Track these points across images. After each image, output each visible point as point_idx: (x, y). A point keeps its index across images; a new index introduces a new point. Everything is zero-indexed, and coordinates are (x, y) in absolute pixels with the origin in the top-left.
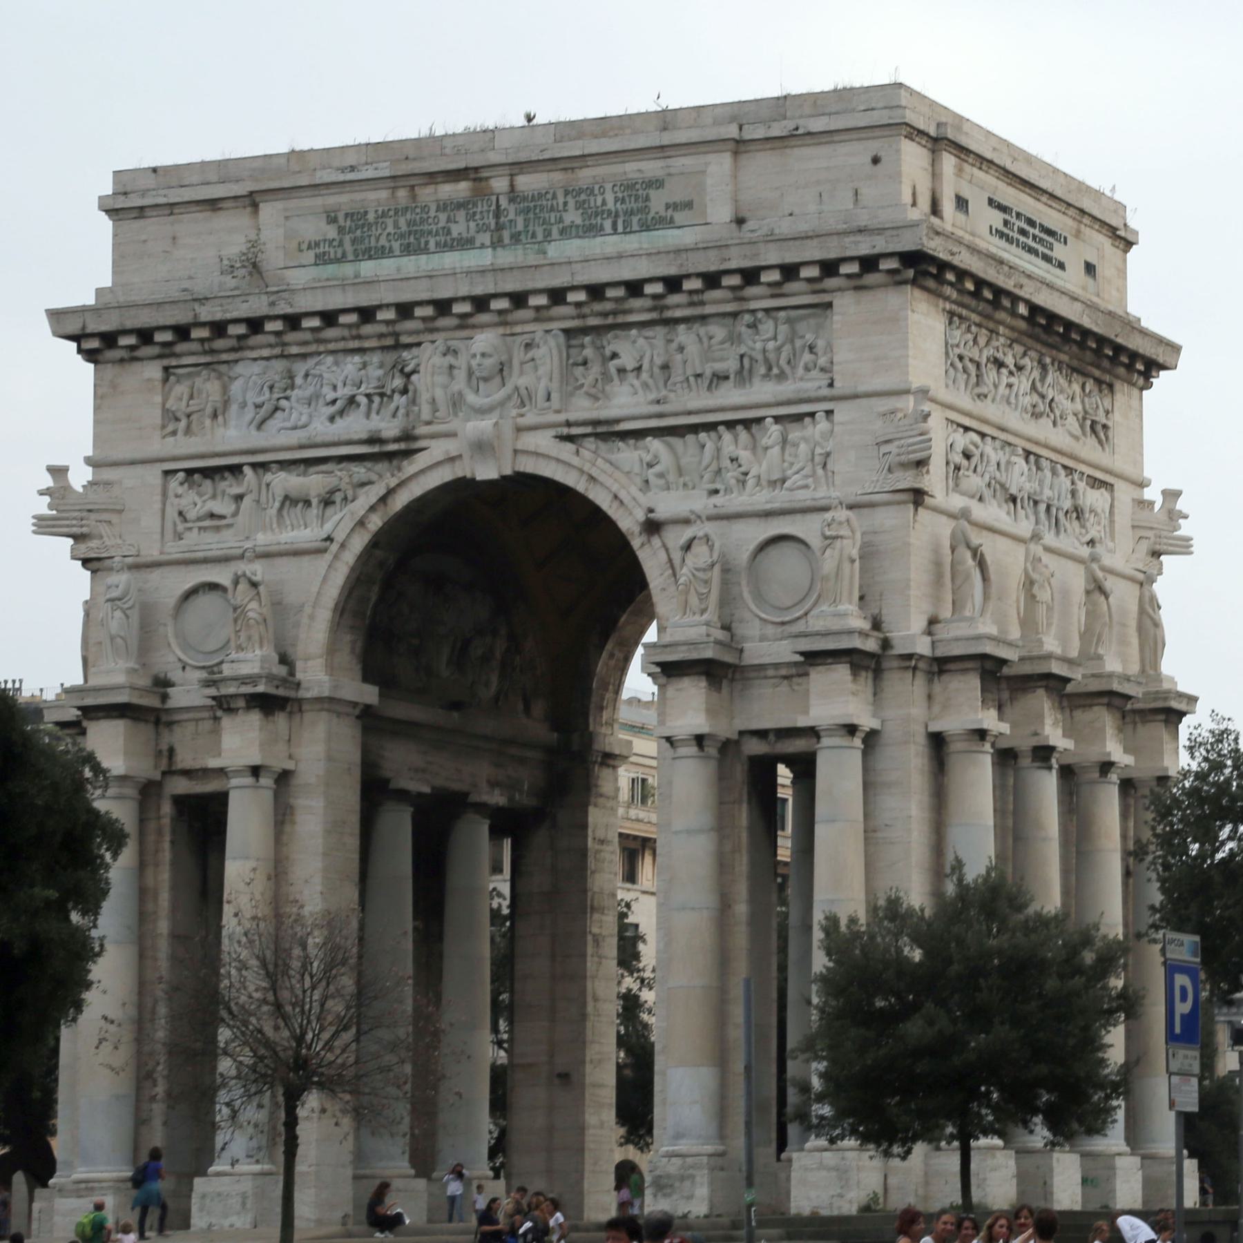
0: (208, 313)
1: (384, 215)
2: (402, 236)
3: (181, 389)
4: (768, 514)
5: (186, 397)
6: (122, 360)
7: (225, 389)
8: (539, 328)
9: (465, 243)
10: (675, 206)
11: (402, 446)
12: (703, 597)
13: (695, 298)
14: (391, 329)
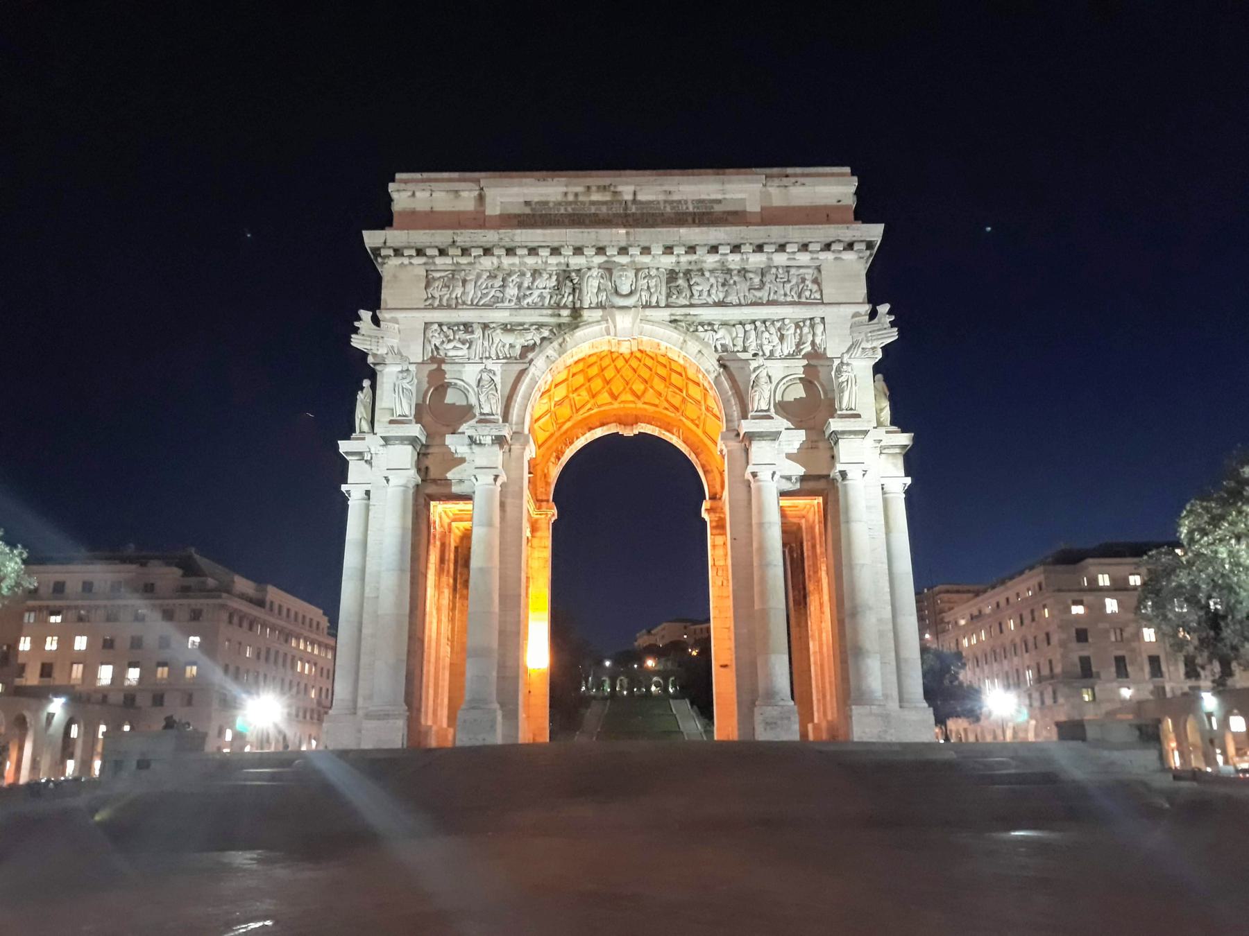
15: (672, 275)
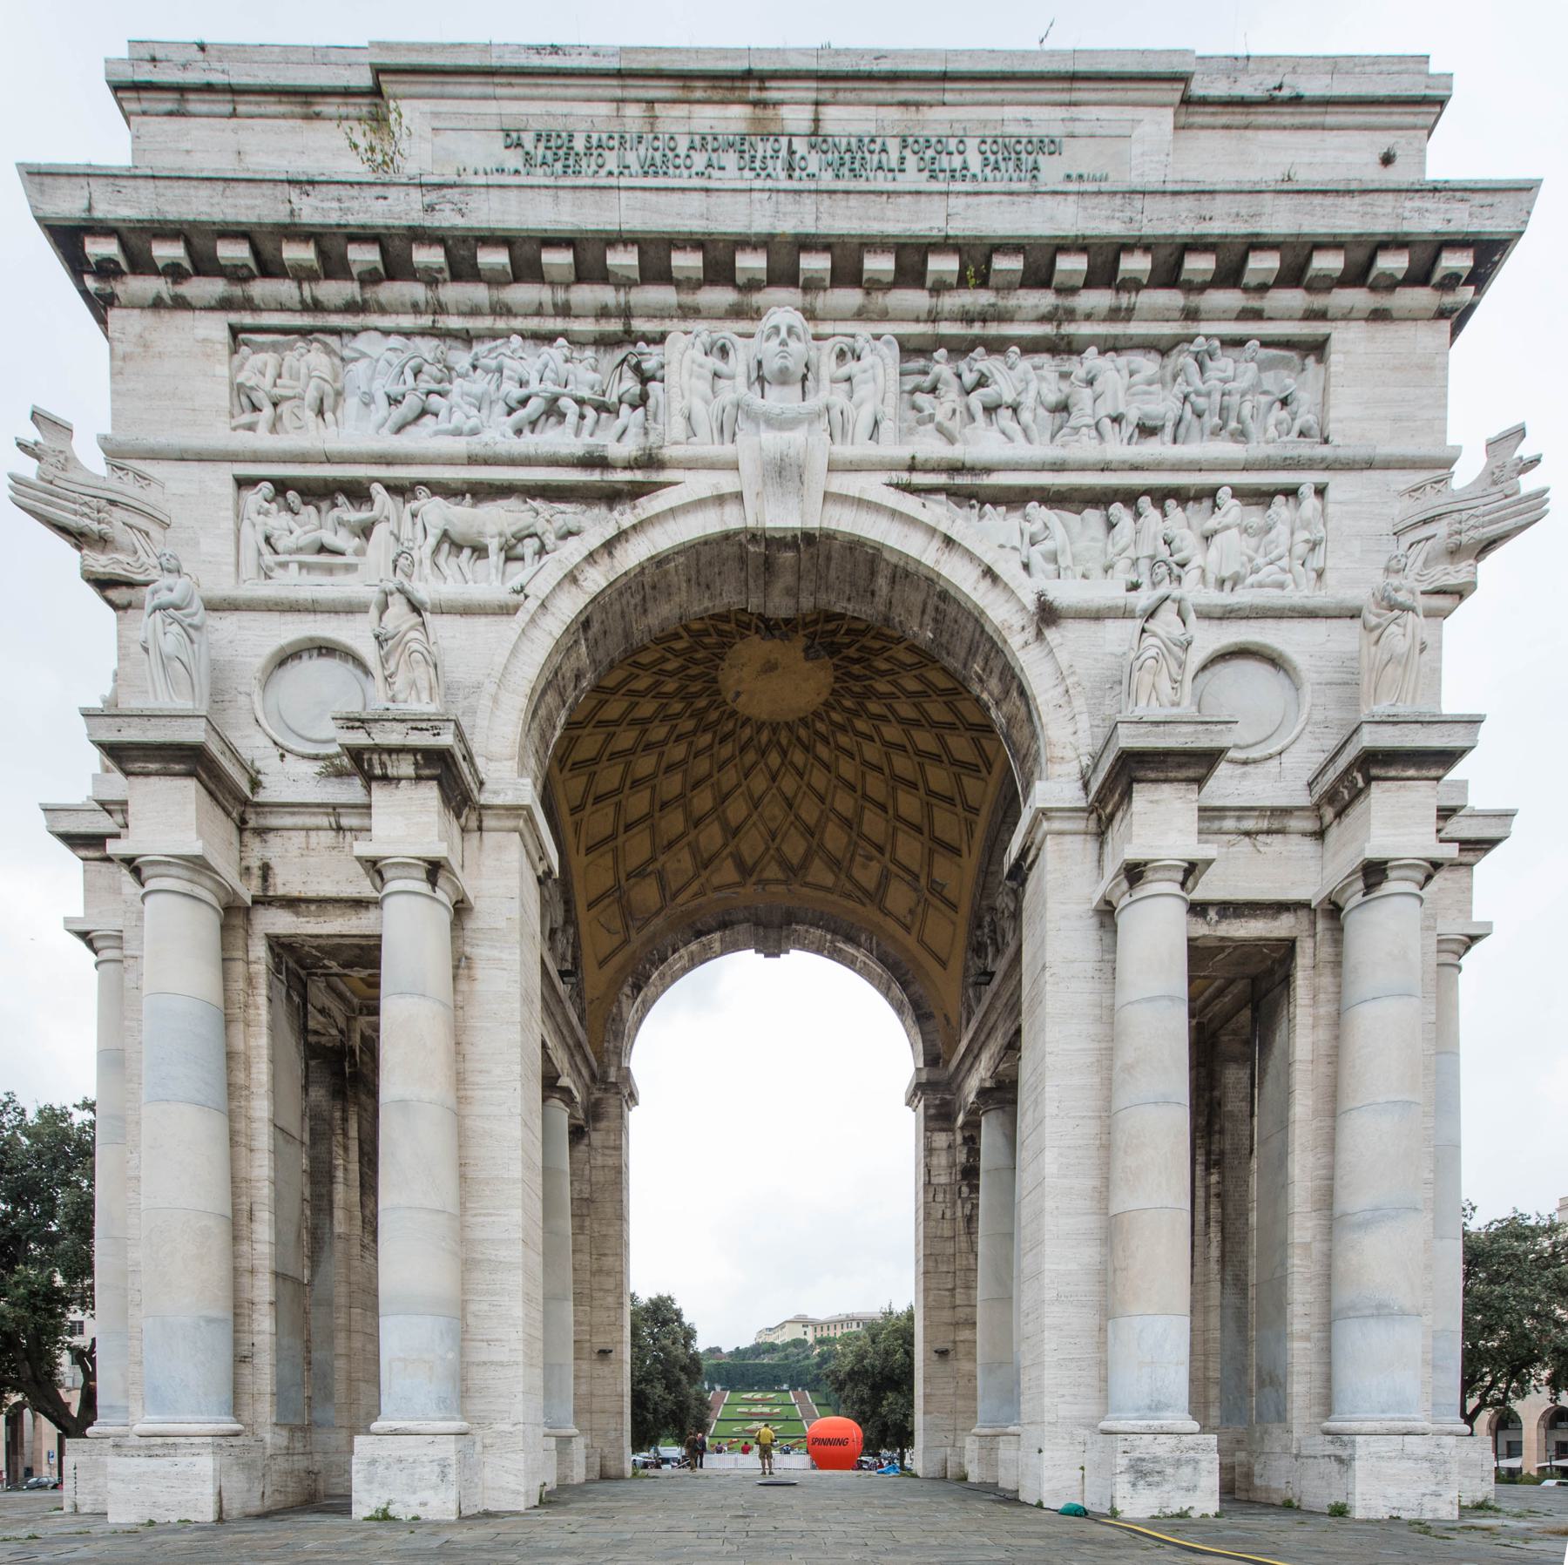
5: (270, 372)
6: (157, 304)
8: (864, 330)
11: (638, 476)
13: (1125, 299)
14: (622, 297)
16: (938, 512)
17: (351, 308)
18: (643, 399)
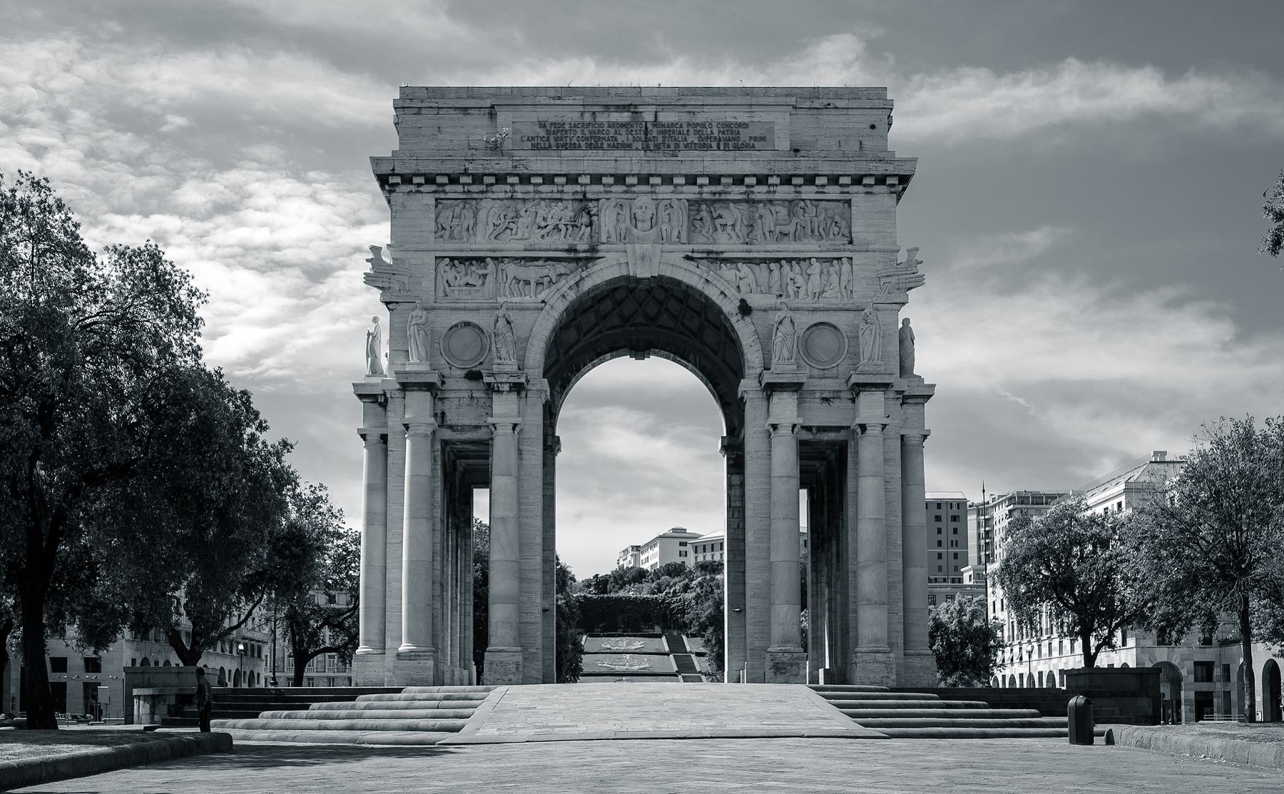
0: (472, 168)
1: (575, 126)
2: (587, 139)
3: (449, 213)
4: (815, 310)
7: (475, 216)
9: (627, 147)
10: (755, 139)
12: (791, 353)
15: (695, 204)
16: (704, 265)
17: (482, 192)
18: (590, 224)
